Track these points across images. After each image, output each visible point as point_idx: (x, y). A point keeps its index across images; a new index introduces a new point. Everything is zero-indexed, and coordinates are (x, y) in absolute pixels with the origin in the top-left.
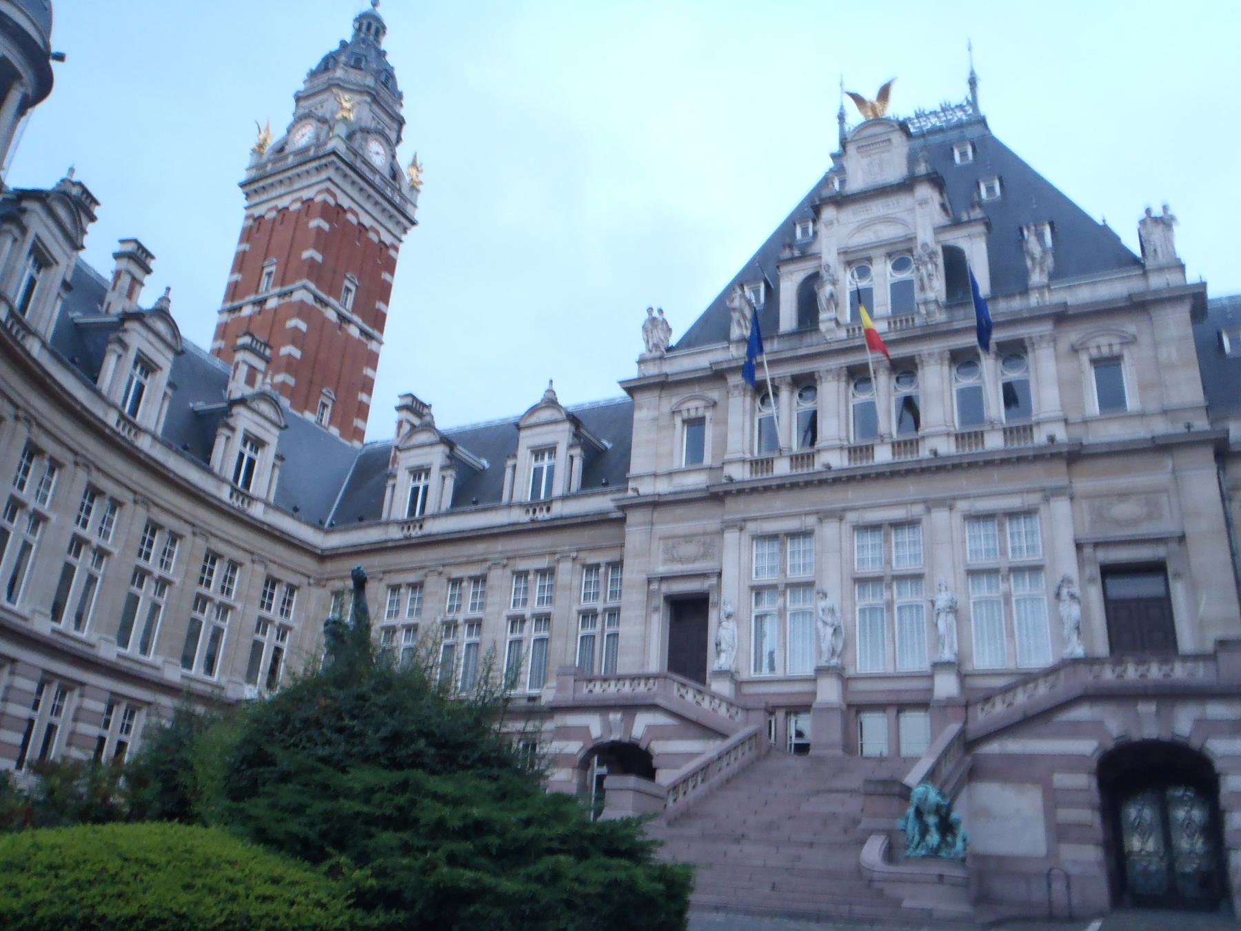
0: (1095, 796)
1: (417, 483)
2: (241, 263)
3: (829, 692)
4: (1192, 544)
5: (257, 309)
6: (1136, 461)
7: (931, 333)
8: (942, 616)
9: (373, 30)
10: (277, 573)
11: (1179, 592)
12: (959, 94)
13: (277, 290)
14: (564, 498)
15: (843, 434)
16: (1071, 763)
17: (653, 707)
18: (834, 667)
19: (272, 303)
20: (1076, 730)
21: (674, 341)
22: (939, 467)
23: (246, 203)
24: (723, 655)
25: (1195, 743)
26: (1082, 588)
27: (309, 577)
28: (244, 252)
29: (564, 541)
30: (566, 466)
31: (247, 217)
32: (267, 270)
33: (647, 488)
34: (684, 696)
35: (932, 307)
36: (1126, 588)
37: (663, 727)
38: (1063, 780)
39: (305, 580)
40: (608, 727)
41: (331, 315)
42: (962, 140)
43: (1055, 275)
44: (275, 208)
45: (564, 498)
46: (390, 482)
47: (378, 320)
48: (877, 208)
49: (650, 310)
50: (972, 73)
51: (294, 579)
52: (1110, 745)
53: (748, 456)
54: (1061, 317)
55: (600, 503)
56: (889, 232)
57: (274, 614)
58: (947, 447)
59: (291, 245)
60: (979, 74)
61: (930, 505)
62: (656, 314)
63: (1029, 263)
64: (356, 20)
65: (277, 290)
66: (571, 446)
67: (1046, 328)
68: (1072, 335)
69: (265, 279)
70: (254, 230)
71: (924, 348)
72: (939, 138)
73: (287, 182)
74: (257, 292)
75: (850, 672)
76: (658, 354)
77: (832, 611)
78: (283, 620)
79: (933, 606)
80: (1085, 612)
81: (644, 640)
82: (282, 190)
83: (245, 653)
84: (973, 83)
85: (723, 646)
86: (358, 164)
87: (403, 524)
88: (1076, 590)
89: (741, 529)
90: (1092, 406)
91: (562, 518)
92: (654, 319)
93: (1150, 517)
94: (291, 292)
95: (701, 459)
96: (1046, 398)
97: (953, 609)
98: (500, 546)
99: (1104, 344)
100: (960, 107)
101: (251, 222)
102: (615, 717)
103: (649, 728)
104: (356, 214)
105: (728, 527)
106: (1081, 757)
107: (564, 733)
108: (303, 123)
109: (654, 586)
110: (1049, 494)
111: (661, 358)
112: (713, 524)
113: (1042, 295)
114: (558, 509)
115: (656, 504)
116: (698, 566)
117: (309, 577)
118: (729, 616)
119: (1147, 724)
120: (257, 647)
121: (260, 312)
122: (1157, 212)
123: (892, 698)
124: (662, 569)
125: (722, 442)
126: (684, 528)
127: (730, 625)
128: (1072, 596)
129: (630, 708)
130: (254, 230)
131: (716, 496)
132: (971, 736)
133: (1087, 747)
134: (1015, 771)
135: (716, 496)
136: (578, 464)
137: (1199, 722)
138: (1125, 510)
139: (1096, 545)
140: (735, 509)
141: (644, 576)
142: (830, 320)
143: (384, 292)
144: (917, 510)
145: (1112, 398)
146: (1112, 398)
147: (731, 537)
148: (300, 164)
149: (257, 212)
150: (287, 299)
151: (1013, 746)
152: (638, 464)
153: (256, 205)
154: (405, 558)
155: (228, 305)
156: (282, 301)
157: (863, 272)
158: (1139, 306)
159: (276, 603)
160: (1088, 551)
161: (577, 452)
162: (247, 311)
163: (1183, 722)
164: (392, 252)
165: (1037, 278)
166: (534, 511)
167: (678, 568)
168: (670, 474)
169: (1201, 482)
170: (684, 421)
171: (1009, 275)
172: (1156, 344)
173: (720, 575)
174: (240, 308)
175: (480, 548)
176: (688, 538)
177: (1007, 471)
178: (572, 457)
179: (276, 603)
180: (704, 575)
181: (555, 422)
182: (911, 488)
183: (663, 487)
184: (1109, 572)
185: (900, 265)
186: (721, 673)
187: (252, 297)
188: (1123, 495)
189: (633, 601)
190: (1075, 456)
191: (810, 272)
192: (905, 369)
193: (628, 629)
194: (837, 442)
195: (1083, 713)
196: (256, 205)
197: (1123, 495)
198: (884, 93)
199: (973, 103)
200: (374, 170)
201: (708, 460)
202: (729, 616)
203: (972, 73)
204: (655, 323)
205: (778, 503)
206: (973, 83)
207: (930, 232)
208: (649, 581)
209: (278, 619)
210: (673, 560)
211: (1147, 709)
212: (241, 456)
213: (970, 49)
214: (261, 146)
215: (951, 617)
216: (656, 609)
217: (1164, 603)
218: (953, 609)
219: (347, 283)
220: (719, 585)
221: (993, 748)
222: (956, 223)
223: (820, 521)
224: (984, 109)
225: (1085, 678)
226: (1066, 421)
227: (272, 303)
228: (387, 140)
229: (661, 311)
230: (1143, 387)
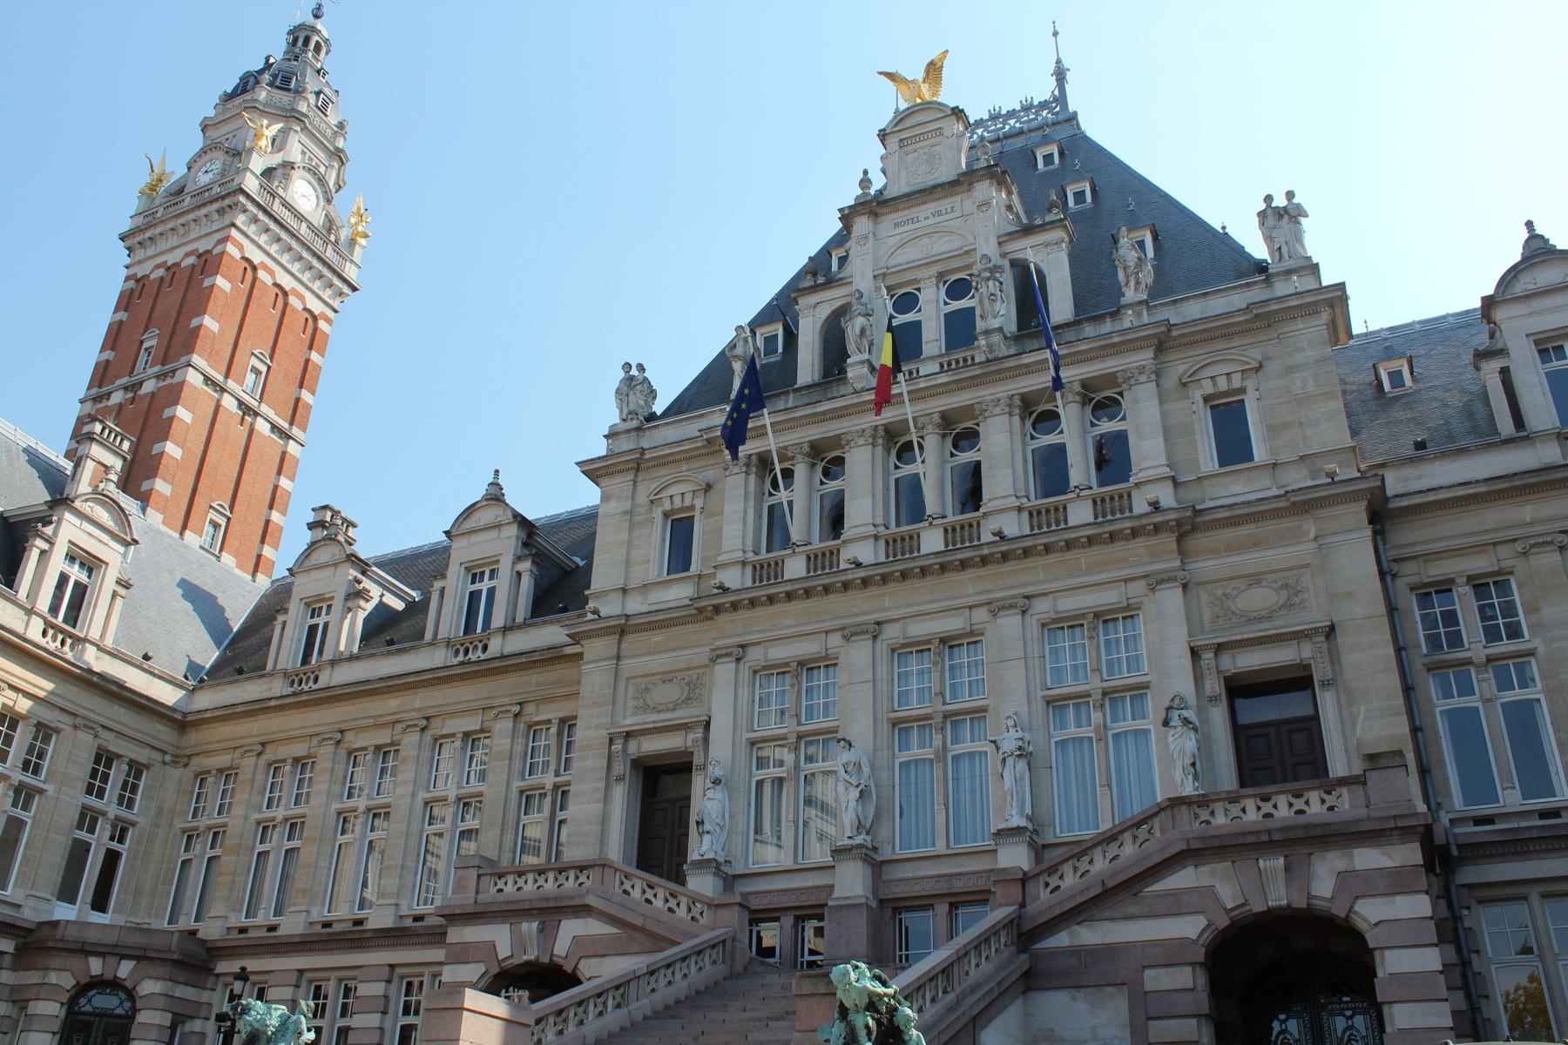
0: (1203, 1001)
1: (315, 621)
2: (114, 337)
3: (852, 883)
4: (1342, 640)
5: (130, 395)
6: (1269, 528)
7: (994, 371)
8: (1010, 761)
9: (312, 46)
10: (115, 745)
12: (1043, 90)
13: (157, 368)
14: (506, 630)
15: (880, 520)
16: (1169, 953)
17: (583, 910)
18: (860, 846)
19: (149, 387)
20: (1176, 905)
21: (659, 407)
22: (1007, 553)
23: (128, 261)
24: (707, 838)
25: (1339, 911)
26: (1200, 710)
27: (164, 752)
28: (121, 322)
29: (503, 689)
30: (512, 585)
31: (127, 279)
32: (145, 345)
33: (610, 608)
34: (646, 896)
35: (996, 338)
36: (1260, 711)
37: (595, 939)
38: (1158, 980)
39: (157, 756)
40: (518, 942)
41: (229, 403)
42: (1046, 141)
43: (1160, 290)
44: (163, 265)
45: (506, 630)
46: (281, 618)
47: (296, 412)
48: (925, 213)
49: (627, 366)
50: (1059, 61)
51: (142, 755)
52: (1223, 922)
53: (750, 556)
54: (1163, 343)
55: (550, 634)
56: (943, 245)
57: (109, 805)
58: (1013, 526)
59: (179, 313)
60: (1066, 64)
61: (997, 608)
62: (634, 372)
63: (1121, 276)
64: (290, 32)
65: (157, 368)
66: (519, 559)
67: (1145, 357)
68: (1178, 367)
69: (143, 356)
70: (136, 295)
72: (1018, 143)
73: (181, 230)
74: (131, 373)
75: (886, 854)
76: (635, 423)
77: (858, 765)
78: (124, 813)
79: (998, 748)
80: (1205, 745)
81: (600, 819)
82: (173, 241)
83: (56, 858)
84: (1060, 75)
85: (707, 827)
86: (277, 207)
87: (291, 677)
88: (1190, 714)
89: (738, 660)
90: (1207, 457)
91: (503, 657)
92: (632, 378)
93: (1288, 606)
94: (174, 372)
95: (686, 568)
96: (1148, 454)
97: (1022, 753)
98: (421, 700)
99: (1220, 376)
100: (1044, 105)
101: (132, 284)
102: (530, 927)
104: (271, 273)
105: (719, 656)
106: (1183, 942)
108: (208, 156)
109: (617, 747)
110: (1156, 582)
111: (638, 429)
112: (701, 655)
113: (1139, 315)
114: (496, 645)
115: (623, 628)
116: (681, 716)
117: (164, 752)
118: (717, 782)
119: (1271, 887)
120: (79, 852)
121: (133, 400)
122: (1280, 201)
123: (943, 888)
124: (630, 722)
125: (716, 538)
126: (660, 662)
127: (717, 794)
128: (1186, 721)
129: (550, 913)
130: (136, 295)
131: (708, 609)
132: (1028, 925)
133: (1190, 927)
134: (1085, 974)
135: (708, 609)
136: (527, 582)
137: (1343, 877)
138: (1259, 598)
139: (1219, 648)
140: (730, 629)
141: (604, 733)
142: (862, 362)
143: (305, 376)
144: (981, 615)
145: (1234, 447)
146: (1234, 447)
147: (725, 670)
148: (198, 207)
149: (140, 271)
150: (168, 381)
151: (1089, 935)
152: (603, 576)
153: (140, 262)
154: (294, 721)
155: (94, 391)
156: (162, 384)
157: (906, 302)
158: (1263, 320)
159: (112, 788)
160: (1208, 656)
161: (526, 566)
162: (117, 398)
163: (1323, 880)
164: (322, 324)
165: (1130, 295)
166: (467, 652)
167: (651, 719)
168: (645, 588)
169: (1354, 553)
170: (666, 515)
171: (1097, 295)
173: (707, 725)
174: (109, 394)
175: (392, 703)
176: (668, 677)
177: (1097, 552)
178: (519, 574)
179: (112, 788)
180: (685, 727)
181: (498, 526)
182: (969, 586)
183: (635, 605)
184: (1239, 689)
185: (958, 289)
186: (702, 864)
187: (124, 380)
188: (1255, 579)
189: (588, 765)
190: (1187, 527)
191: (839, 303)
193: (581, 809)
194: (871, 530)
195: (1184, 878)
196: (140, 262)
197: (1255, 579)
198: (934, 70)
199: (1061, 99)
200: (300, 217)
201: (694, 568)
202: (717, 782)
203: (1059, 61)
204: (634, 384)
205: (790, 616)
206: (1060, 75)
207: (993, 242)
208: (611, 741)
209: (113, 810)
210: (646, 708)
211: (1275, 863)
212: (63, 579)
213: (1055, 34)
214: (152, 188)
215: (1022, 765)
216: (620, 779)
217: (1311, 726)
218: (1022, 753)
219: (254, 361)
220: (706, 740)
221: (1061, 940)
222: (1027, 230)
223: (847, 638)
225: (1188, 826)
226: (1173, 479)
227: (149, 387)
228: (321, 181)
229: (641, 368)
230: (1273, 430)
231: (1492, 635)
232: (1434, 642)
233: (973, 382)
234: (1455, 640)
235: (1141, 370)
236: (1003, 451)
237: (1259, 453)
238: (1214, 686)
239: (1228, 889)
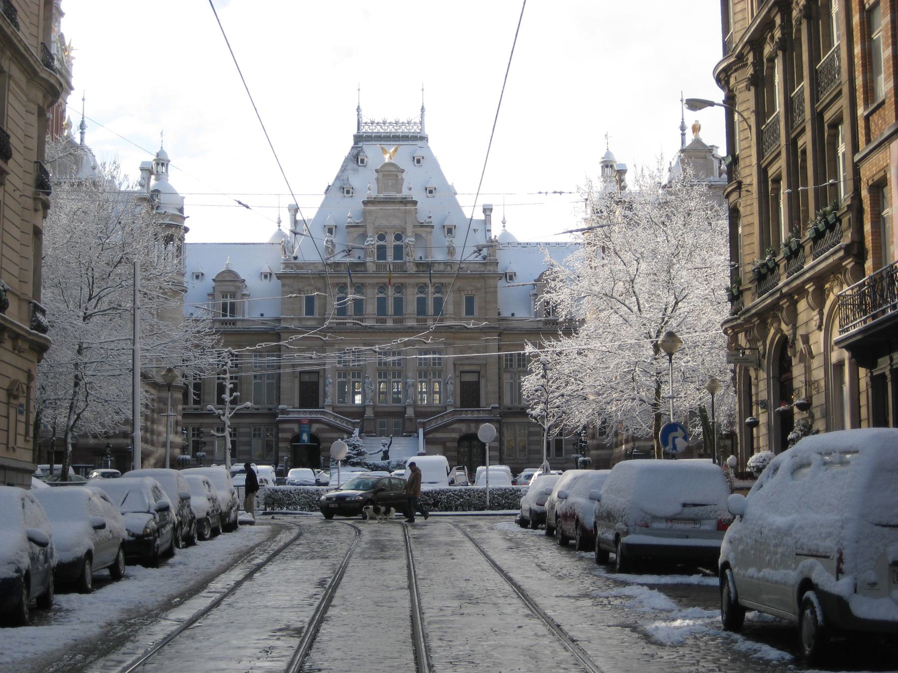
11: (482, 382)
20: (454, 431)
38: (449, 444)
71: (407, 281)
80: (455, 388)
96: (449, 307)
103: (318, 429)
107: (285, 431)
133: (456, 435)
145: (470, 311)
172: (486, 292)
192: (400, 288)
195: (456, 426)
201: (316, 315)
221: (431, 436)
224: (428, 131)
231: (519, 366)
232: (506, 365)
233: (405, 277)
234: (511, 366)
235: (449, 284)
236: (411, 298)
237: (476, 314)
238: (458, 373)
239: (463, 427)
